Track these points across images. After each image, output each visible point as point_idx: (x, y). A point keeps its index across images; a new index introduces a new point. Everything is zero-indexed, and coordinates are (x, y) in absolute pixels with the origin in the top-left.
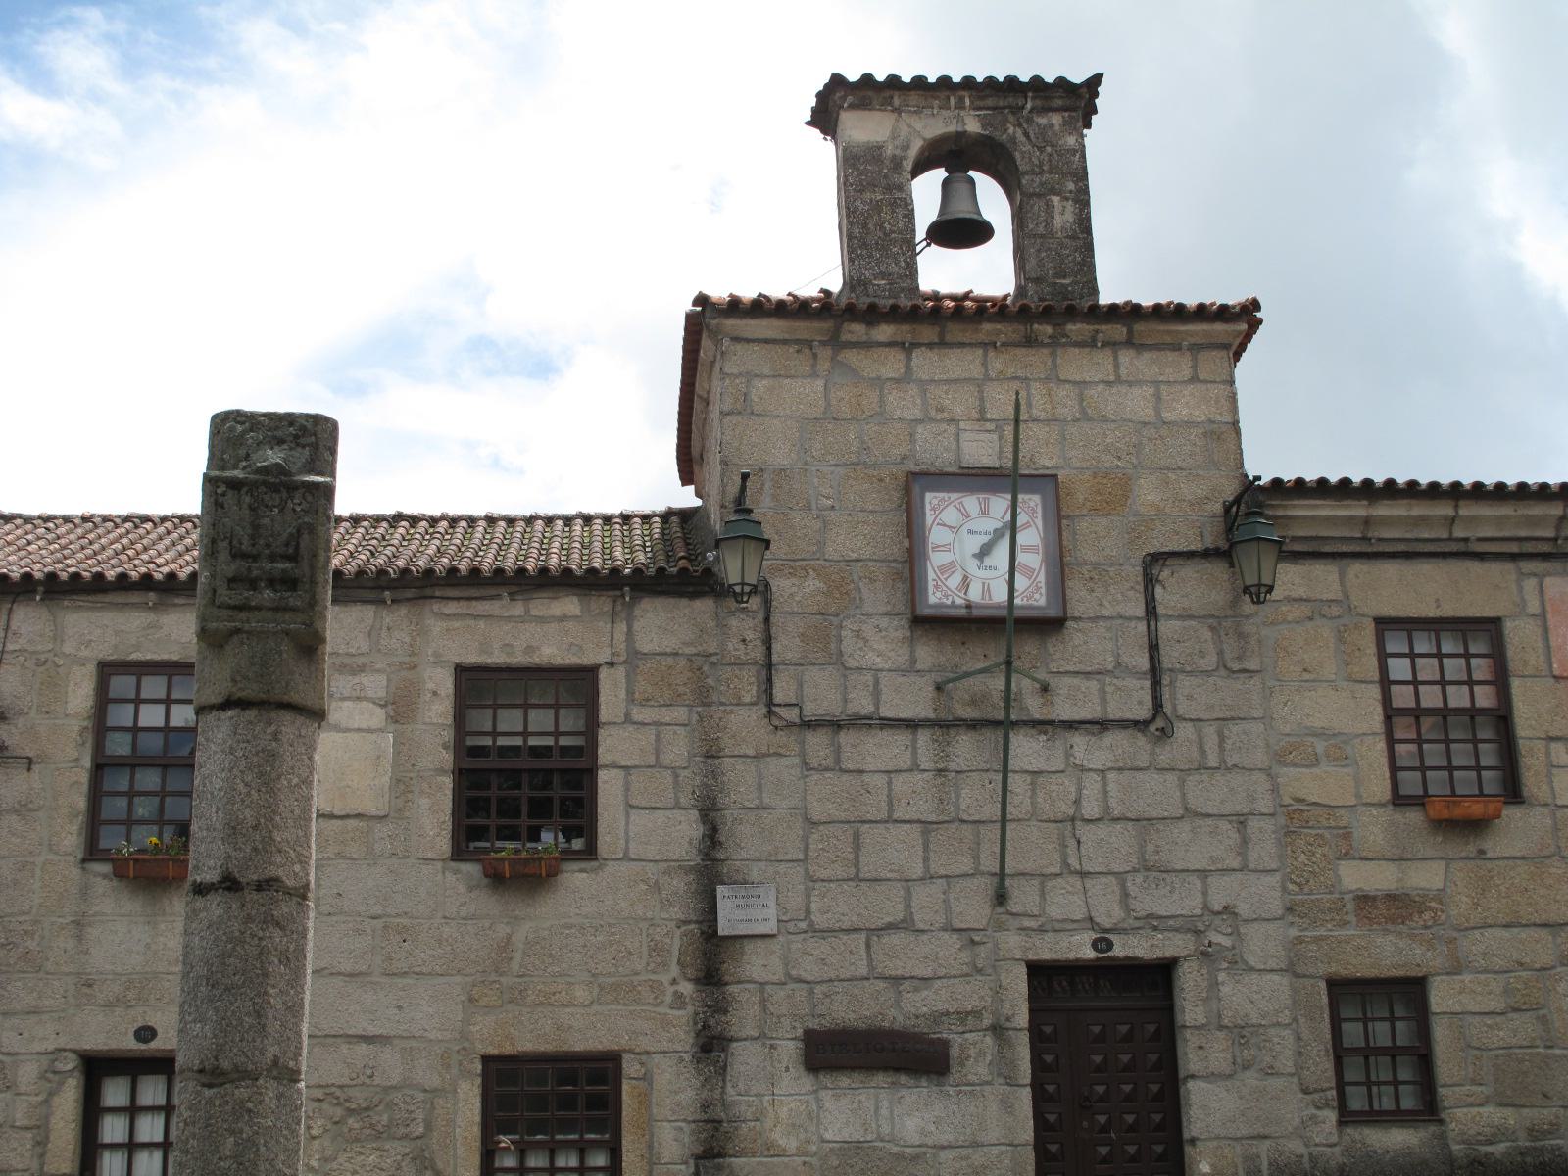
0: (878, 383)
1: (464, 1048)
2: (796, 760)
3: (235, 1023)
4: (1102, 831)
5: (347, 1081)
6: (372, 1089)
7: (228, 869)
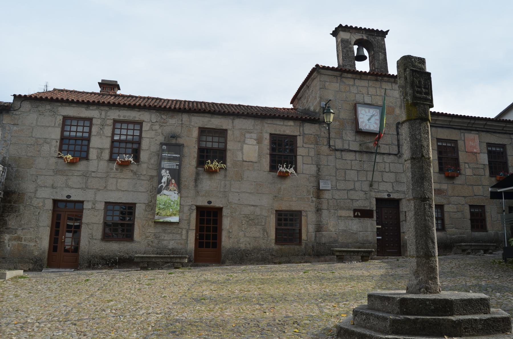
0: (349, 85)
2: (334, 157)
4: (389, 174)
5: (249, 214)
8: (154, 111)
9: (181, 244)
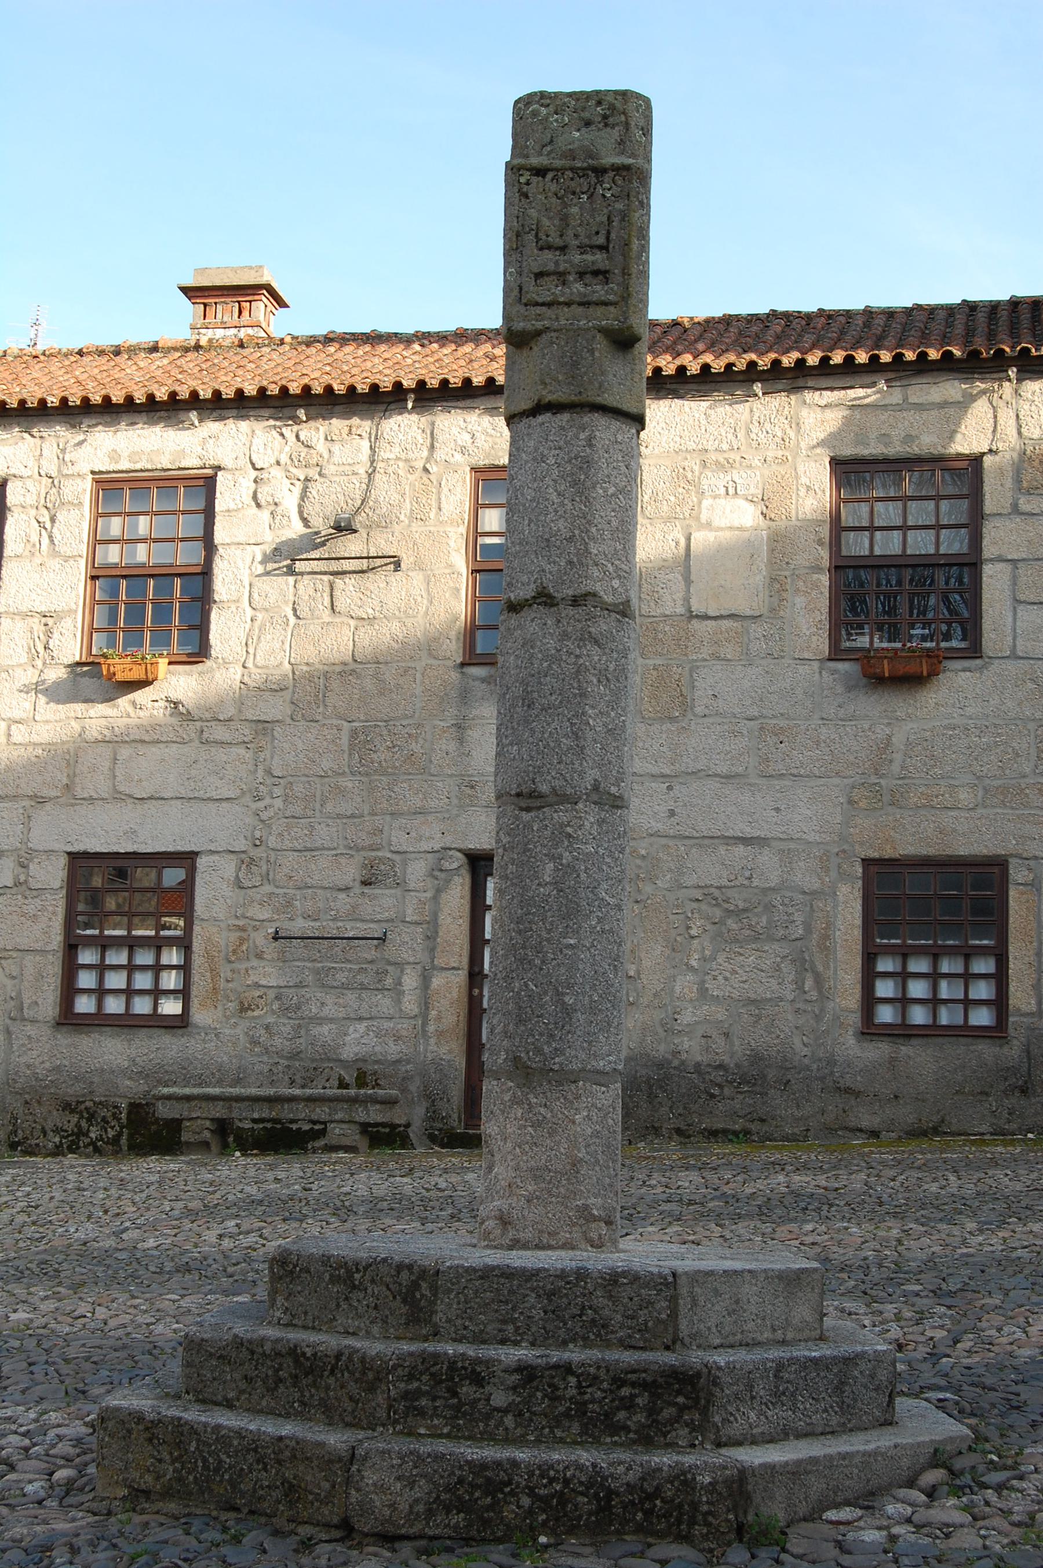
1: (844, 851)
3: (552, 744)
6: (750, 890)
7: (542, 583)
8: (266, 412)
9: (398, 1038)
